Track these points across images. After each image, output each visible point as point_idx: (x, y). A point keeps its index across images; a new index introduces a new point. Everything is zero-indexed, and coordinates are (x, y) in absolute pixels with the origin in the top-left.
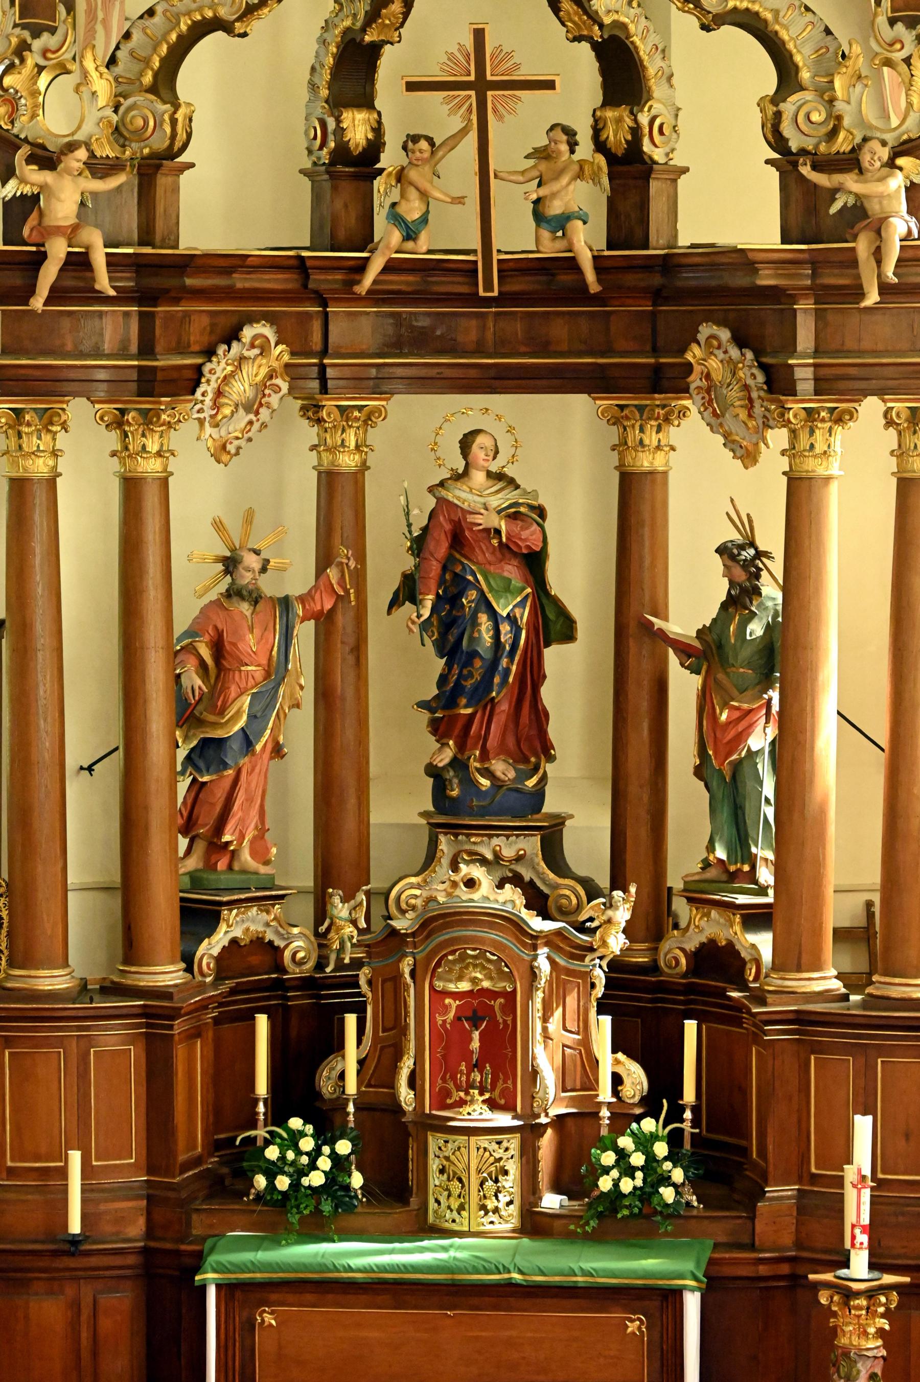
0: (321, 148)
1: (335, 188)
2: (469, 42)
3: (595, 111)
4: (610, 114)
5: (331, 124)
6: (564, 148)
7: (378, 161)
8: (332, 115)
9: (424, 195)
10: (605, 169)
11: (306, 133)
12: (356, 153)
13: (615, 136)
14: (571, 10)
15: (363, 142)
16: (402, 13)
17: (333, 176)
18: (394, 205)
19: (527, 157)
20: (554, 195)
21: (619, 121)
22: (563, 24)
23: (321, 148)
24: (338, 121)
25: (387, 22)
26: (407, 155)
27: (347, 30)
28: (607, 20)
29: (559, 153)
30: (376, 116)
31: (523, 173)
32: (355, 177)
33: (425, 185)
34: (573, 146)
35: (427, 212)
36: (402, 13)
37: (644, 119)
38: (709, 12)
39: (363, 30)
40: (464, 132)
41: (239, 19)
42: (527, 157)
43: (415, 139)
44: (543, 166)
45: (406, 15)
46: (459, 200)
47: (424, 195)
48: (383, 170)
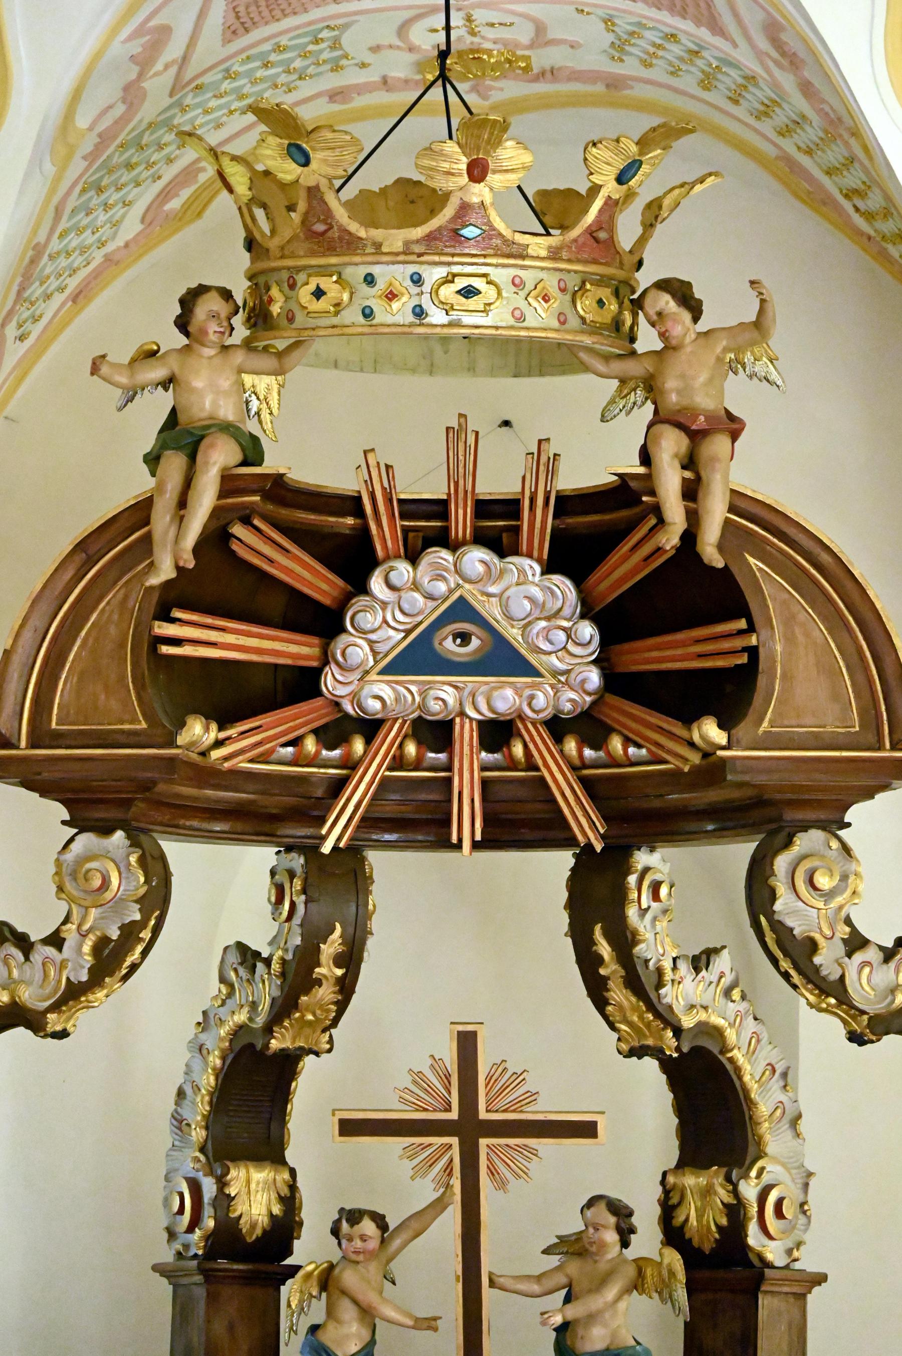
0: (190, 1229)
1: (212, 1298)
2: (449, 1055)
3: (665, 1174)
4: (691, 1180)
5: (209, 1187)
6: (611, 1237)
7: (289, 1252)
8: (211, 1173)
9: (367, 1314)
10: (681, 1275)
11: (167, 1202)
12: (250, 1239)
13: (699, 1217)
14: (625, 1003)
15: (263, 1221)
16: (336, 1003)
17: (209, 1276)
18: (314, 1329)
19: (546, 1252)
20: (591, 1318)
21: (707, 1192)
22: (612, 1026)
23: (190, 1229)
24: (222, 1183)
25: (310, 1017)
26: (340, 1244)
27: (240, 1029)
28: (688, 1022)
29: (603, 1246)
30: (286, 1176)
31: (539, 1278)
32: (247, 1279)
33: (370, 1297)
34: (625, 1234)
35: (372, 1342)
36: (336, 1003)
37: (749, 1190)
38: (863, 1012)
39: (268, 1030)
40: (438, 1206)
41: (56, 1007)
42: (546, 1252)
43: (354, 1216)
44: (574, 1268)
45: (342, 1006)
46: (429, 1324)
47: (367, 1314)
48: (297, 1268)
